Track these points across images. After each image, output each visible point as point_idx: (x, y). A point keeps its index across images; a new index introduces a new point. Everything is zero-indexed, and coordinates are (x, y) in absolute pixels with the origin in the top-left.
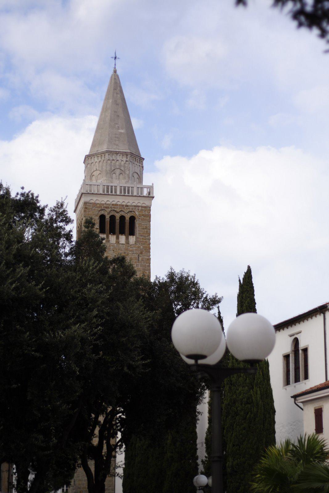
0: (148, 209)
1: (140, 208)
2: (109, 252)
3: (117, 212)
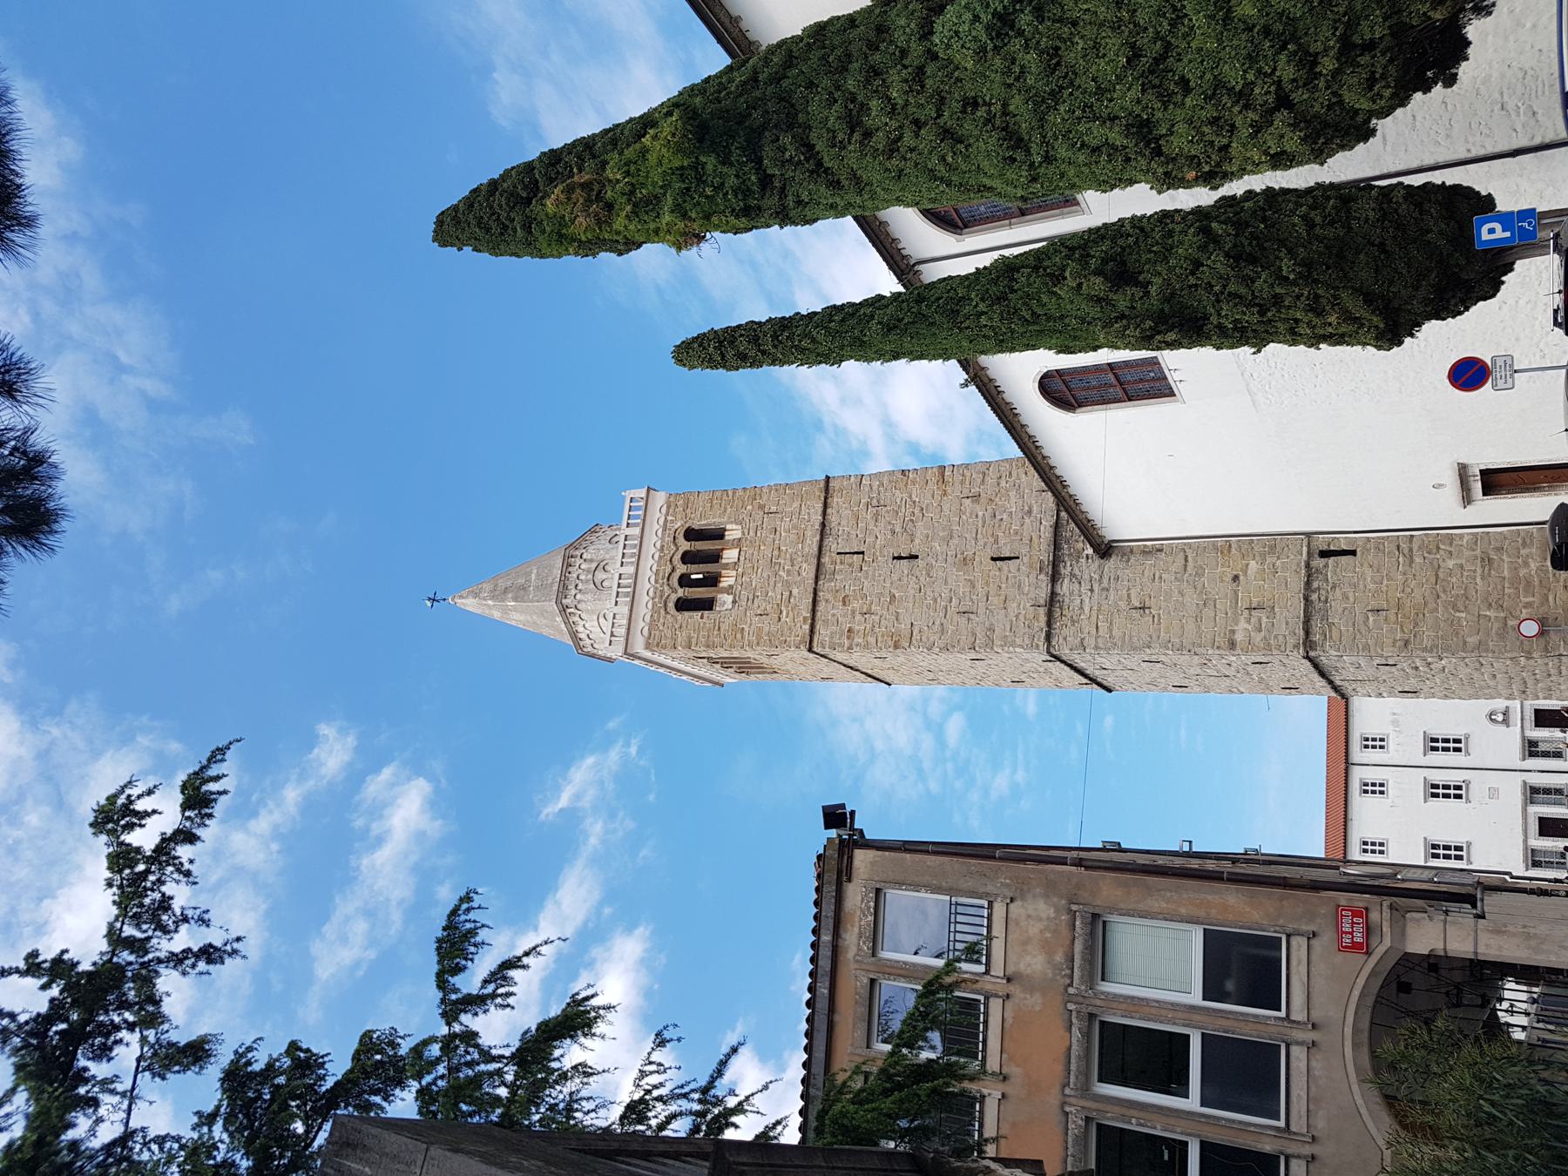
3: (673, 570)
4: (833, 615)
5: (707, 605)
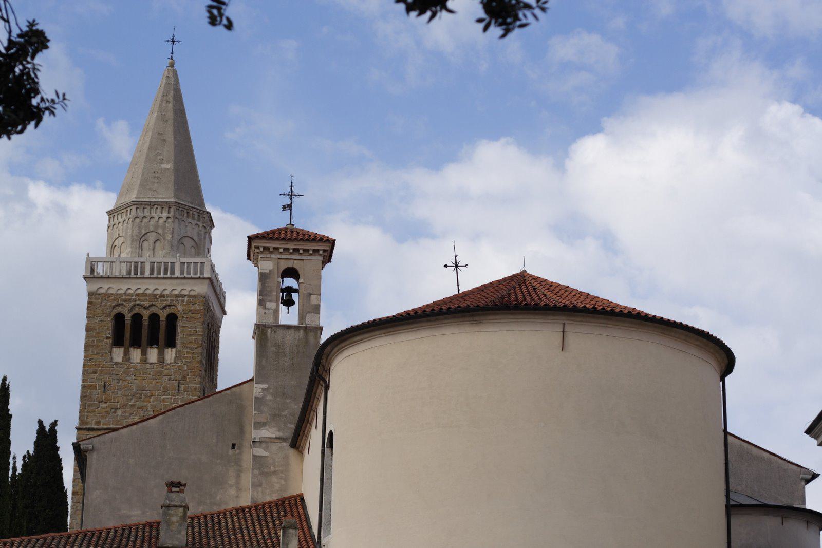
1: (186, 299)
2: (127, 378)
3: (145, 308)
5: (118, 341)
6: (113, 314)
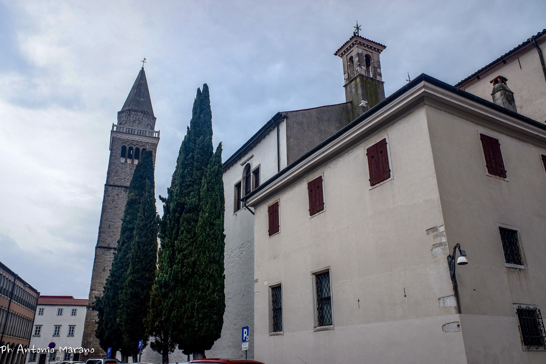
0: (156, 145)
1: (150, 144)
3: (134, 145)
4: (114, 191)
6: (122, 146)
